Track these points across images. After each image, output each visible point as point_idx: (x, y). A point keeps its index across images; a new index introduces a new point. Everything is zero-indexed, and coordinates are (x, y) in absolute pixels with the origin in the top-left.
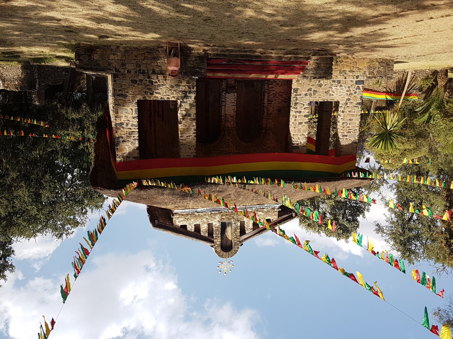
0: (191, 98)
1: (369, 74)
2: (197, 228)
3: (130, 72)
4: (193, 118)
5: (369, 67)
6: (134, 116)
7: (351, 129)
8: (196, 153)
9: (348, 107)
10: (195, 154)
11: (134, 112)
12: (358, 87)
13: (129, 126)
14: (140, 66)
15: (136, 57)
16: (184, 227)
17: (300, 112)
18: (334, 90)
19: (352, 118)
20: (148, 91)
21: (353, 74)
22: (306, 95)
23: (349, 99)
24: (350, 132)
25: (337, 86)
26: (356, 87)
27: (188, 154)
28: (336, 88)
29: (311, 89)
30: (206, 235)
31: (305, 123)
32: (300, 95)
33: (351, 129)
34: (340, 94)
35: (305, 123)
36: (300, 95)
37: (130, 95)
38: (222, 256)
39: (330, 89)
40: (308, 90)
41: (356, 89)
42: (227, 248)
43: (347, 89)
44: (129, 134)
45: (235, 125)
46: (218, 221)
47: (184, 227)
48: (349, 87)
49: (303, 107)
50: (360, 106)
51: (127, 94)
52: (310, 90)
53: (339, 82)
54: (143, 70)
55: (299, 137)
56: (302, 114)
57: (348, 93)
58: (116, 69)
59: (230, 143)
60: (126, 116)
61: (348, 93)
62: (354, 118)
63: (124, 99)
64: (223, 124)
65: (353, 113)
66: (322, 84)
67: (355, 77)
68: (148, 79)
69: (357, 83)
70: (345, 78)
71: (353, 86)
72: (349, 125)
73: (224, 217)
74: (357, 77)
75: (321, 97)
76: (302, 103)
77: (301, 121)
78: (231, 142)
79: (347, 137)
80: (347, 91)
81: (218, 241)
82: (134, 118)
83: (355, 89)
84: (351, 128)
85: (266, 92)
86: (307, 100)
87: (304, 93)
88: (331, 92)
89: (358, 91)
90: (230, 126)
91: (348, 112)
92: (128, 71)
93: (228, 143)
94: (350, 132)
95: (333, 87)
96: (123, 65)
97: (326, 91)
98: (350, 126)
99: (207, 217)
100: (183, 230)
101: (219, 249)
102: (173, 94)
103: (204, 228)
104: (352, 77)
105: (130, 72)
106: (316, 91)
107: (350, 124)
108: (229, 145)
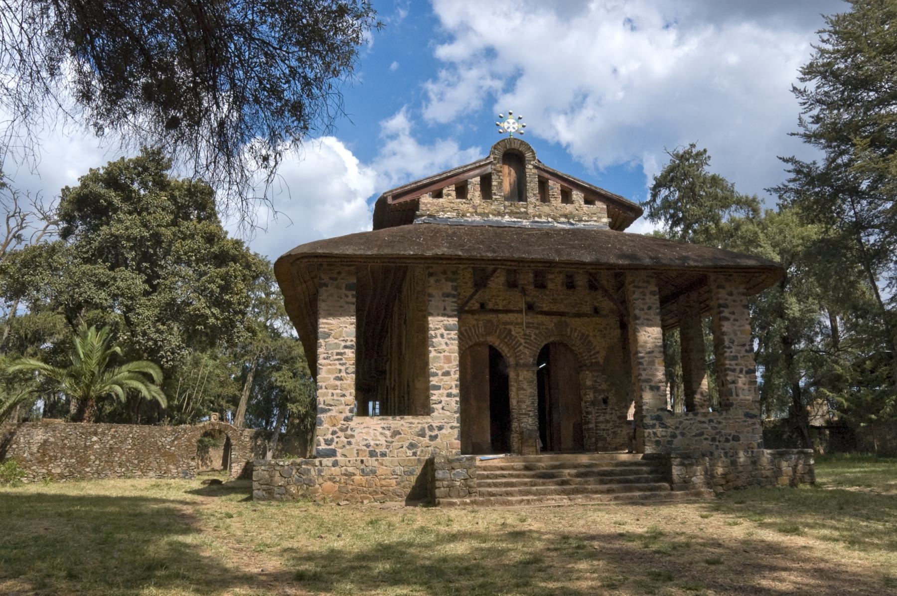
1: (309, 470)
2: (566, 197)
5: (310, 483)
6: (732, 386)
7: (338, 360)
11: (734, 390)
12: (329, 445)
13: (738, 368)
17: (449, 395)
19: (338, 383)
21: (346, 470)
22: (440, 428)
24: (338, 354)
25: (377, 445)
26: (334, 444)
28: (378, 442)
30: (551, 183)
31: (437, 375)
32: (452, 428)
33: (338, 360)
35: (436, 375)
36: (452, 428)
39: (390, 439)
40: (436, 437)
41: (332, 440)
48: (349, 443)
49: (443, 404)
52: (433, 438)
53: (372, 454)
55: (447, 348)
56: (446, 392)
57: (349, 432)
59: (522, 341)
61: (349, 432)
62: (333, 382)
64: (535, 377)
65: (335, 392)
66: (409, 449)
69: (333, 453)
70: (362, 461)
71: (340, 445)
72: (343, 368)
73: (523, 210)
74: (335, 464)
75: (407, 424)
77: (446, 378)
78: (521, 344)
79: (343, 344)
80: (353, 436)
83: (336, 440)
84: (337, 362)
87: (444, 431)
89: (329, 437)
91: (347, 393)
94: (338, 354)
95: (385, 443)
97: (397, 437)
98: (339, 367)
100: (592, 195)
101: (528, 155)
102: (681, 423)
106: (419, 435)
107: (340, 371)
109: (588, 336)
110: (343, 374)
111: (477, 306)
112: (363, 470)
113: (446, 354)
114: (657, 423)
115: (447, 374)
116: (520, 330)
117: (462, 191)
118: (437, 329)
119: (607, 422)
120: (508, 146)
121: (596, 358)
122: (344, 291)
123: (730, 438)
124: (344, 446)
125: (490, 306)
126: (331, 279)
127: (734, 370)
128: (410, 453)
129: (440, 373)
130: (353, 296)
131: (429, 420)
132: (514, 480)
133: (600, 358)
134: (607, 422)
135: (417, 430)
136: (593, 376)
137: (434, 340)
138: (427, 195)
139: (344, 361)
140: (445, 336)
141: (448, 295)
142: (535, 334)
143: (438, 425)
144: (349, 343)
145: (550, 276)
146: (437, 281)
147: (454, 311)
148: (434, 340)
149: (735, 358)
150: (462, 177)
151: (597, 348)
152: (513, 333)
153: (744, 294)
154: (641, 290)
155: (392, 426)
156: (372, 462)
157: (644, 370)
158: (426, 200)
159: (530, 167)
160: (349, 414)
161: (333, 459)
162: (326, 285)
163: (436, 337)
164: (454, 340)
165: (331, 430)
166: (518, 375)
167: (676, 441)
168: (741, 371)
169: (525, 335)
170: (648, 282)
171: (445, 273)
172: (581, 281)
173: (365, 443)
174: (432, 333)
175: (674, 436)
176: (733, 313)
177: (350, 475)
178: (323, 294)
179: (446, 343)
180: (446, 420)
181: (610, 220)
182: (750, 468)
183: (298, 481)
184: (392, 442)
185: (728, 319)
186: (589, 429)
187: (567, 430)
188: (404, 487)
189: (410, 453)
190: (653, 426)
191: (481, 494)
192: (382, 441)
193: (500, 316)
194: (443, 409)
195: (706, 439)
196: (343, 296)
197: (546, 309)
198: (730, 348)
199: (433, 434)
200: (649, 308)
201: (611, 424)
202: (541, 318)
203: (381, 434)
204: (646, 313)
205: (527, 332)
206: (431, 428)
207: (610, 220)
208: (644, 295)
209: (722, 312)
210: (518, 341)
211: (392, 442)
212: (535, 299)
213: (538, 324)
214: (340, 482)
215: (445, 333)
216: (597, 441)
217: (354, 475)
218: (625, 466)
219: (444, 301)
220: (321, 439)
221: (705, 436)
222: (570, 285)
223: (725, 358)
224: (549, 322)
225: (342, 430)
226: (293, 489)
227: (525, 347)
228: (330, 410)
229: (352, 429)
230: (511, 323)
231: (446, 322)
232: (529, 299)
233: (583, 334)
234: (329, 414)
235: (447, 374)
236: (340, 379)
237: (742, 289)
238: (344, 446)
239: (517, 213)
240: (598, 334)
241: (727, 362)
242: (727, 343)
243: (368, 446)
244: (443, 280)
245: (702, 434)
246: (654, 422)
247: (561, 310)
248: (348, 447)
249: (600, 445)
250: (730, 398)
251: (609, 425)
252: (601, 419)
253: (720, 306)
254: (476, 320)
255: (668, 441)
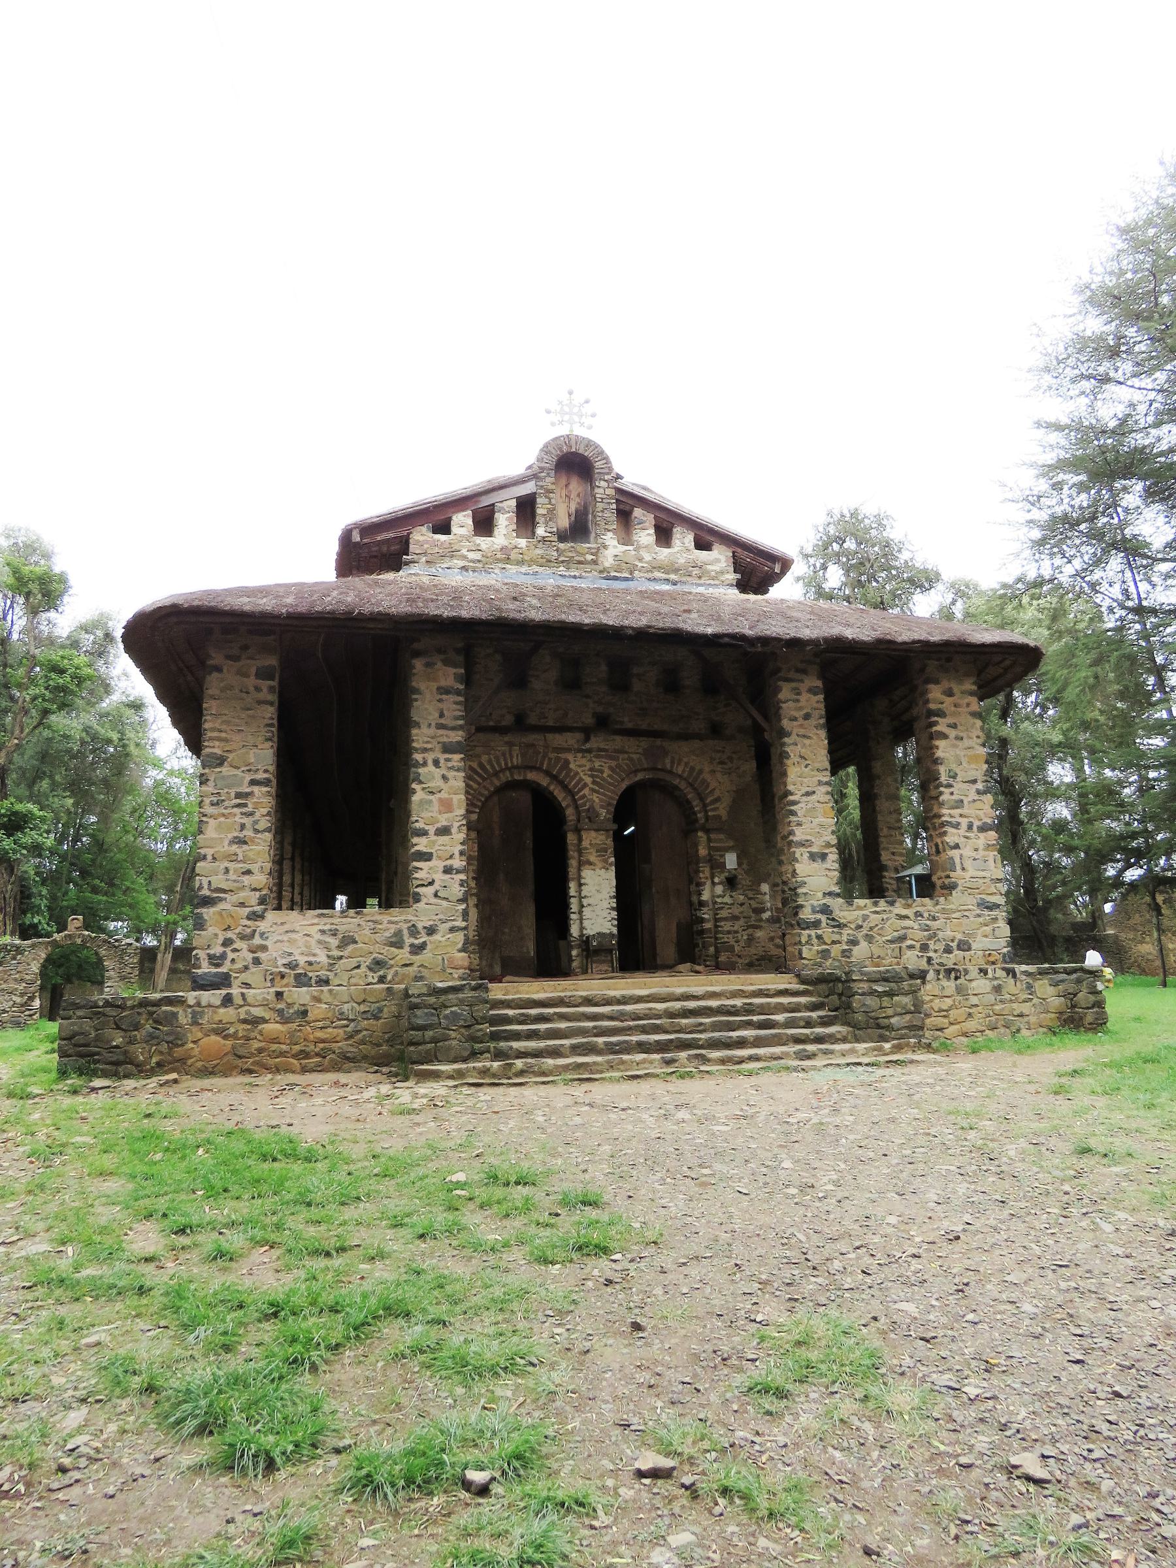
0: (813, 907)
1: (175, 1015)
2: (664, 535)
3: (981, 970)
4: (802, 849)
5: (176, 1040)
6: (955, 854)
7: (238, 806)
8: (784, 744)
9: (255, 890)
10: (786, 740)
11: (957, 861)
12: (218, 965)
13: (964, 822)
14: (960, 990)
15: (970, 1014)
16: (702, 545)
17: (448, 870)
18: (318, 951)
20: (928, 922)
21: (248, 1013)
22: (431, 931)
23: (255, 916)
24: (239, 795)
25: (310, 964)
26: (227, 963)
27: (807, 742)
29: (413, 953)
30: (638, 512)
32: (452, 930)
33: (238, 806)
34: (293, 936)
35: (423, 833)
37: (970, 907)
38: (589, 443)
39: (336, 953)
40: (423, 946)
41: (223, 956)
42: (575, 463)
43: (262, 955)
44: (962, 801)
45: (571, 838)
46: (605, 547)
47: (702, 545)
48: (257, 962)
49: (436, 886)
50: (205, 892)
51: (978, 912)
52: (418, 949)
53: (302, 980)
54: (949, 978)
57: (257, 941)
58: (1014, 976)
59: (588, 780)
60: (976, 850)
61: (257, 941)
62: (226, 848)
63: (983, 896)
64: (610, 842)
65: (231, 866)
67: (238, 1000)
68: (931, 954)
69: (224, 981)
71: (239, 965)
72: (247, 821)
73: (589, 557)
74: (227, 1000)
76: (444, 903)
78: (585, 785)
79: (248, 777)
80: (264, 948)
81: (602, 489)
82: (957, 846)
83: (231, 956)
84: (237, 810)
85: (472, 944)
86: (424, 912)
87: (437, 937)
88: (334, 942)
89: (217, 950)
90: (593, 834)
91: (255, 868)
92: (986, 973)
93: (594, 782)
94: (239, 795)
96: (997, 989)
97: (351, 947)
99: (640, 565)
102: (865, 918)
103: (646, 536)
104: (249, 1000)
105: (981, 970)
106: (392, 944)
108: (592, 776)
109: (701, 772)
110: (248, 833)
111: (508, 720)
112: (280, 1012)
113: (443, 795)
114: (823, 918)
115: (444, 831)
116: (584, 761)
117: (484, 524)
118: (425, 750)
119: (735, 918)
120: (565, 449)
121: (713, 810)
122: (252, 681)
123: (954, 945)
124: (246, 968)
125: (533, 720)
126: (228, 657)
127: (957, 826)
128: (373, 977)
129: (432, 830)
130: (271, 689)
131: (410, 917)
132: (563, 1025)
133: (722, 810)
134: (735, 918)
135: (387, 934)
136: (709, 840)
137: (420, 770)
138: (424, 529)
139: (250, 809)
140: (442, 761)
141: (447, 691)
142: (611, 768)
143: (428, 924)
144: (261, 776)
145: (636, 670)
146: (428, 665)
147: (457, 718)
148: (420, 770)
149: (959, 804)
150: (485, 501)
151: (717, 793)
152: (572, 766)
153: (972, 694)
154: (794, 685)
155: (341, 928)
156: (300, 996)
157: (799, 824)
158: (421, 536)
159: (603, 484)
160: (259, 908)
161: (224, 992)
162: (218, 669)
163: (425, 764)
164: (458, 770)
165: (220, 940)
166: (580, 840)
167: (856, 950)
168: (970, 827)
169: (591, 770)
170: (804, 672)
171: (440, 651)
172: (690, 677)
173: (285, 961)
174: (418, 757)
175: (854, 942)
176: (954, 726)
177: (256, 1021)
178: (213, 684)
179: (444, 777)
180: (441, 916)
181: (739, 576)
182: (991, 998)
183: (152, 1037)
184: (341, 958)
185: (945, 736)
186: (702, 932)
187: (665, 933)
188: (363, 1042)
189: (373, 977)
190: (816, 924)
191: (499, 1055)
192: (322, 958)
193: (550, 736)
194: (436, 895)
195: (911, 947)
196: (252, 689)
197: (630, 726)
198: (949, 786)
199: (416, 942)
200: (807, 717)
201: (742, 922)
202: (619, 741)
203: (319, 942)
204: (801, 726)
205: (597, 764)
206: (414, 931)
207: (739, 576)
208: (798, 694)
209: (935, 723)
210: (581, 779)
211: (341, 958)
212: (611, 710)
213: (616, 751)
214: (235, 1036)
215: (442, 757)
216: (717, 951)
217: (265, 1021)
218: (767, 996)
219: (440, 701)
220: (202, 954)
221: (909, 942)
222: (671, 684)
223: (941, 804)
224: (635, 748)
225: (243, 937)
226: (139, 1052)
227: (593, 790)
228: (221, 900)
229: (262, 935)
230: (568, 750)
231: (441, 740)
232: (600, 709)
233: (692, 769)
234: (221, 906)
235: (444, 831)
236: (242, 842)
237: (969, 686)
238: (246, 968)
239: (580, 562)
240: (719, 768)
241: (944, 811)
242: (943, 778)
243: (292, 966)
244: (439, 665)
245: (903, 938)
246: (819, 916)
247: (656, 727)
248: (253, 969)
249: (723, 958)
250: (952, 874)
251: (738, 925)
252: (724, 913)
253: (931, 713)
254: (506, 743)
255: (844, 951)
